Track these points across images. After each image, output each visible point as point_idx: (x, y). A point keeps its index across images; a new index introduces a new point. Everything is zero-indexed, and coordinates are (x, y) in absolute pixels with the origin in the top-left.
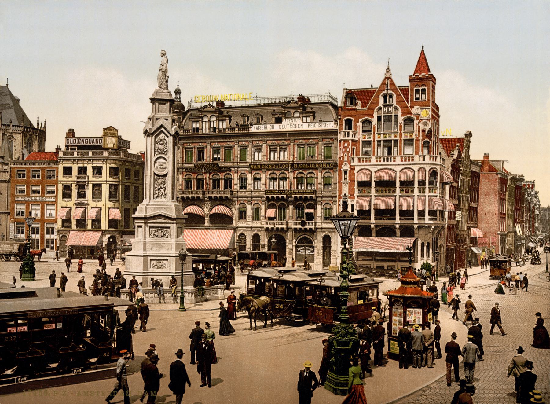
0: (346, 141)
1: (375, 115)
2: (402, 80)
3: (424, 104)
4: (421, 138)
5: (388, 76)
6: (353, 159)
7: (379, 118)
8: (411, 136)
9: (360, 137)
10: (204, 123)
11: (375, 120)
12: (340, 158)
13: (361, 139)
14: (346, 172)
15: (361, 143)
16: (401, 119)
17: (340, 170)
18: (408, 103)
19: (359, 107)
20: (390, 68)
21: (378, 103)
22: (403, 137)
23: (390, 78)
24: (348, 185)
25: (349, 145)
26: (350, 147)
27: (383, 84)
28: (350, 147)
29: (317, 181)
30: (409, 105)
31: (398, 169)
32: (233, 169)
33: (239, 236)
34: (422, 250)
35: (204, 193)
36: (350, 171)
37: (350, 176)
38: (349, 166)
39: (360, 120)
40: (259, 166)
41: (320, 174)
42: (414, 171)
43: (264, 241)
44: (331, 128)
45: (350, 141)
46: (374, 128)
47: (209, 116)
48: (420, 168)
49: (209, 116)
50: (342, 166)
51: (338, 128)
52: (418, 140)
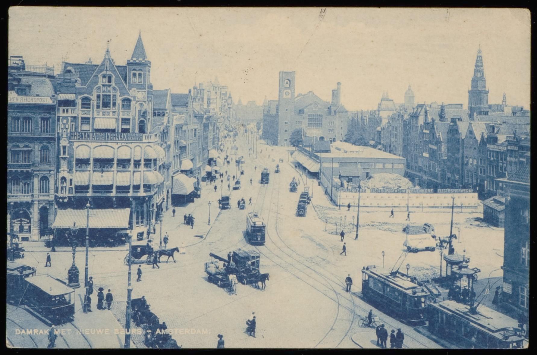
0: (66, 118)
1: (95, 94)
3: (141, 87)
4: (137, 118)
7: (98, 97)
11: (94, 98)
13: (81, 115)
14: (64, 147)
22: (121, 116)
25: (68, 121)
38: (68, 142)
39: (80, 97)
46: (93, 105)
52: (134, 119)
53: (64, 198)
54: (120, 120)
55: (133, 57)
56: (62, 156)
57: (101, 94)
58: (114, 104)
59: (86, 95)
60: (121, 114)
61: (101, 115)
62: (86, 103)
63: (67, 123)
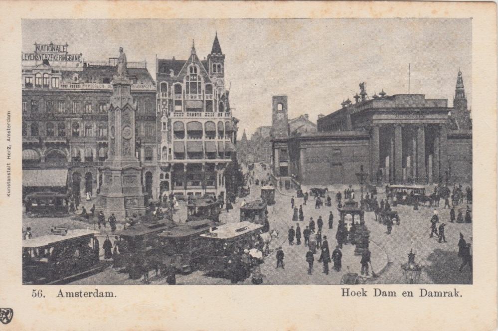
0: (164, 100)
1: (185, 81)
2: (203, 55)
4: (218, 100)
5: (193, 53)
6: (169, 114)
8: (211, 98)
9: (174, 97)
10: (37, 79)
12: (158, 113)
13: (174, 99)
15: (174, 102)
16: (203, 87)
17: (159, 123)
18: (209, 74)
19: (172, 75)
20: (195, 47)
21: (187, 72)
22: (205, 99)
23: (195, 54)
24: (166, 134)
26: (168, 104)
27: (190, 59)
28: (168, 104)
29: (140, 130)
30: (209, 76)
31: (203, 122)
32: (67, 119)
33: (75, 173)
34: (220, 182)
35: (40, 139)
36: (168, 123)
37: (168, 126)
39: (174, 84)
40: (90, 118)
41: (142, 124)
42: (214, 123)
43: (96, 177)
44: (151, 89)
45: (168, 100)
47: (42, 72)
48: (219, 122)
49: (42, 72)
50: (162, 119)
51: (156, 89)
52: (216, 101)
53: (165, 163)
54: (205, 102)
55: (213, 52)
56: (162, 130)
57: (189, 81)
58: (200, 91)
59: (178, 83)
60: (205, 98)
61: (190, 98)
62: (178, 90)
63: (166, 105)
